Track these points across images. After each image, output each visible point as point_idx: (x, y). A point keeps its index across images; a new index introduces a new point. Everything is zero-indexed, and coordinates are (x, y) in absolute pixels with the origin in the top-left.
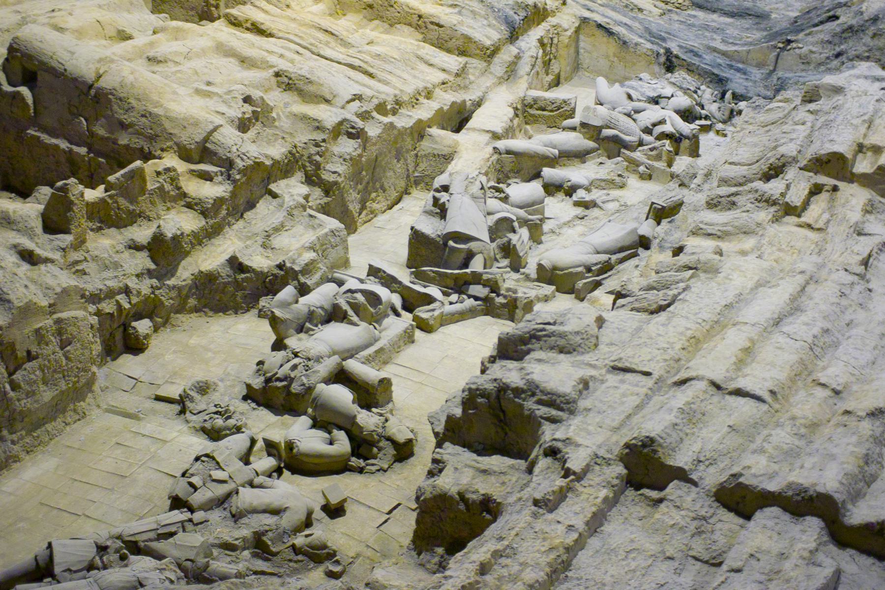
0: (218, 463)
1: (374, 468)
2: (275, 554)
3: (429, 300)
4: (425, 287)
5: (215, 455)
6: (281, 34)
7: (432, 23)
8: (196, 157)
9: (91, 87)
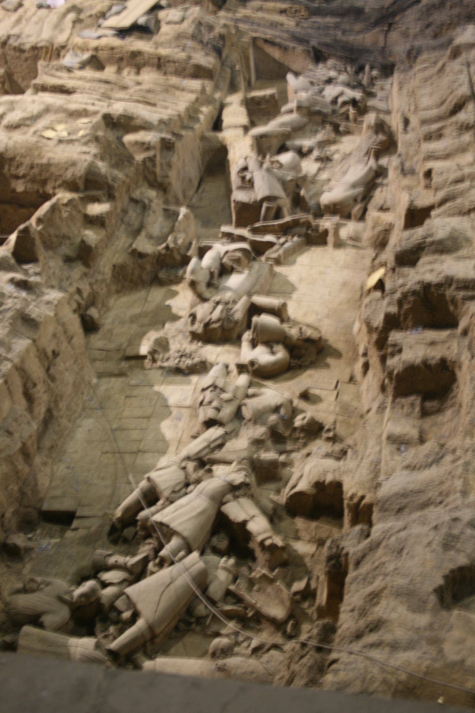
3: (271, 245)
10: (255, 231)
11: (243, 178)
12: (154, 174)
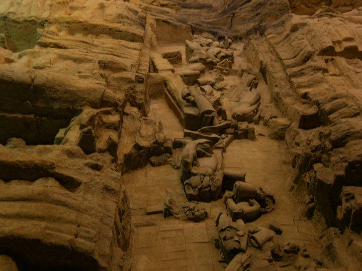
1: (270, 210)
2: (282, 257)
3: (216, 140)
6: (70, 47)
7: (116, 31)
8: (99, 106)
9: (30, 85)
10: (203, 131)
11: (188, 101)
12: (134, 98)
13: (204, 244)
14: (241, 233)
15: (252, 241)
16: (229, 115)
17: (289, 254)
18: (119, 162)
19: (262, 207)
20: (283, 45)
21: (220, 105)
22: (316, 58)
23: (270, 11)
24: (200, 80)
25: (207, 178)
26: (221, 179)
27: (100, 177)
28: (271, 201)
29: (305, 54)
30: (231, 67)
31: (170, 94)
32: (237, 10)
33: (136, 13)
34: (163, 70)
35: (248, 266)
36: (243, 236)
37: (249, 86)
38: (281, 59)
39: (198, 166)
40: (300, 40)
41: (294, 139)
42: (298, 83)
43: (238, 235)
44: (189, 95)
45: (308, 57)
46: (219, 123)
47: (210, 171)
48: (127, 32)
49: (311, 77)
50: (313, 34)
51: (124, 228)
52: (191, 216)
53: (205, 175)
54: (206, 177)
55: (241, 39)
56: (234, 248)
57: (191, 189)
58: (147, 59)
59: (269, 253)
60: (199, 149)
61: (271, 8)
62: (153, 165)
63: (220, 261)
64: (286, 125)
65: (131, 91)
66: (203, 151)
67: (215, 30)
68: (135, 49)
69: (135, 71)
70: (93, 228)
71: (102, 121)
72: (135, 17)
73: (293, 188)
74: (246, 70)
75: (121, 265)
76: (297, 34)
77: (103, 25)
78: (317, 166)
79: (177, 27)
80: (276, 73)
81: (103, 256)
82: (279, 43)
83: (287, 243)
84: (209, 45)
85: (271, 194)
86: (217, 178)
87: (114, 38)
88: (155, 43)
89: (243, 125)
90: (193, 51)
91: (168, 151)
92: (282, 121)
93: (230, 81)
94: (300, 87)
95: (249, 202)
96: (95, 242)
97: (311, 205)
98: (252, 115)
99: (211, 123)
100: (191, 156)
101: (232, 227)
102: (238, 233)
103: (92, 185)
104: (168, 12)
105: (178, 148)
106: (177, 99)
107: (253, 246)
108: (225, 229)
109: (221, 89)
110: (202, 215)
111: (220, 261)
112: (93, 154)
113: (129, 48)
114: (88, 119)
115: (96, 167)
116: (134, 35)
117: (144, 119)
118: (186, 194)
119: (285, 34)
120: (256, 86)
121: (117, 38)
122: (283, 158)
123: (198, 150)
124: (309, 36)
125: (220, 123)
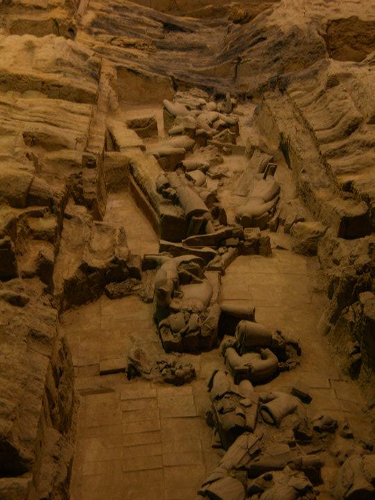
0: (238, 395)
1: (294, 364)
2: (310, 438)
3: (210, 256)
4: (201, 248)
5: (232, 390)
7: (53, 85)
10: (189, 243)
11: (166, 195)
12: (81, 191)
13: (189, 420)
14: (246, 402)
15: (264, 413)
16: (230, 217)
17: (321, 433)
18: (55, 293)
19: (280, 361)
20: (314, 108)
21: (217, 201)
22: (365, 127)
23: (297, 54)
24: (186, 162)
25: (195, 316)
26: (217, 318)
27: (23, 317)
28: (295, 351)
29: (349, 122)
30: (234, 142)
31: (138, 184)
32: (245, 53)
33: (85, 57)
34: (128, 147)
35: (258, 452)
36: (250, 406)
37: (263, 172)
38: (311, 130)
39: (182, 297)
40: (341, 99)
41: (331, 254)
42: (338, 166)
43: (242, 405)
44: (167, 185)
45: (353, 127)
46: (214, 229)
47: (199, 305)
48: (69, 86)
49: (358, 157)
50: (361, 90)
51: (62, 397)
52: (169, 376)
53: (191, 312)
54: (193, 315)
55: (250, 98)
56: (236, 425)
57: (170, 333)
58: (102, 130)
59: (290, 433)
60: (182, 270)
61: (297, 49)
62: (111, 296)
63: (214, 447)
64: (318, 232)
65: (76, 181)
66: (189, 274)
67: (210, 85)
68: (83, 114)
69: (83, 149)
70: (10, 398)
71: (28, 227)
72: (82, 64)
73: (329, 329)
74: (258, 147)
75: (56, 454)
76: (338, 90)
77: (32, 77)
78: (365, 297)
79: (150, 80)
80: (304, 151)
81: (27, 441)
82: (310, 104)
83: (318, 416)
84: (200, 107)
85: (295, 340)
86: (210, 316)
87: (49, 97)
88: (116, 105)
89: (253, 233)
90: (175, 117)
91: (134, 274)
92: (312, 226)
93: (233, 163)
94: (340, 172)
95: (259, 352)
96: (13, 420)
97: (356, 357)
98: (267, 216)
99: (203, 229)
100: (170, 282)
101: (232, 393)
102: (242, 401)
103: (10, 330)
104: (136, 56)
105: (150, 269)
106: (149, 192)
107: (265, 421)
108: (223, 396)
109: (218, 177)
110: (186, 374)
111: (214, 447)
112: (12, 281)
113: (73, 112)
114: (5, 225)
115: (17, 302)
116: (82, 91)
117: (97, 225)
118: (162, 342)
119: (318, 90)
120: (273, 171)
121: (54, 97)
122: (315, 284)
123: (180, 272)
124: (355, 94)
125: (216, 230)
